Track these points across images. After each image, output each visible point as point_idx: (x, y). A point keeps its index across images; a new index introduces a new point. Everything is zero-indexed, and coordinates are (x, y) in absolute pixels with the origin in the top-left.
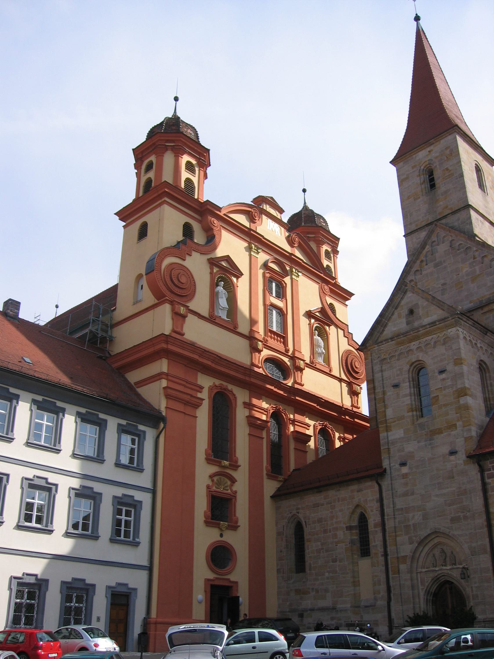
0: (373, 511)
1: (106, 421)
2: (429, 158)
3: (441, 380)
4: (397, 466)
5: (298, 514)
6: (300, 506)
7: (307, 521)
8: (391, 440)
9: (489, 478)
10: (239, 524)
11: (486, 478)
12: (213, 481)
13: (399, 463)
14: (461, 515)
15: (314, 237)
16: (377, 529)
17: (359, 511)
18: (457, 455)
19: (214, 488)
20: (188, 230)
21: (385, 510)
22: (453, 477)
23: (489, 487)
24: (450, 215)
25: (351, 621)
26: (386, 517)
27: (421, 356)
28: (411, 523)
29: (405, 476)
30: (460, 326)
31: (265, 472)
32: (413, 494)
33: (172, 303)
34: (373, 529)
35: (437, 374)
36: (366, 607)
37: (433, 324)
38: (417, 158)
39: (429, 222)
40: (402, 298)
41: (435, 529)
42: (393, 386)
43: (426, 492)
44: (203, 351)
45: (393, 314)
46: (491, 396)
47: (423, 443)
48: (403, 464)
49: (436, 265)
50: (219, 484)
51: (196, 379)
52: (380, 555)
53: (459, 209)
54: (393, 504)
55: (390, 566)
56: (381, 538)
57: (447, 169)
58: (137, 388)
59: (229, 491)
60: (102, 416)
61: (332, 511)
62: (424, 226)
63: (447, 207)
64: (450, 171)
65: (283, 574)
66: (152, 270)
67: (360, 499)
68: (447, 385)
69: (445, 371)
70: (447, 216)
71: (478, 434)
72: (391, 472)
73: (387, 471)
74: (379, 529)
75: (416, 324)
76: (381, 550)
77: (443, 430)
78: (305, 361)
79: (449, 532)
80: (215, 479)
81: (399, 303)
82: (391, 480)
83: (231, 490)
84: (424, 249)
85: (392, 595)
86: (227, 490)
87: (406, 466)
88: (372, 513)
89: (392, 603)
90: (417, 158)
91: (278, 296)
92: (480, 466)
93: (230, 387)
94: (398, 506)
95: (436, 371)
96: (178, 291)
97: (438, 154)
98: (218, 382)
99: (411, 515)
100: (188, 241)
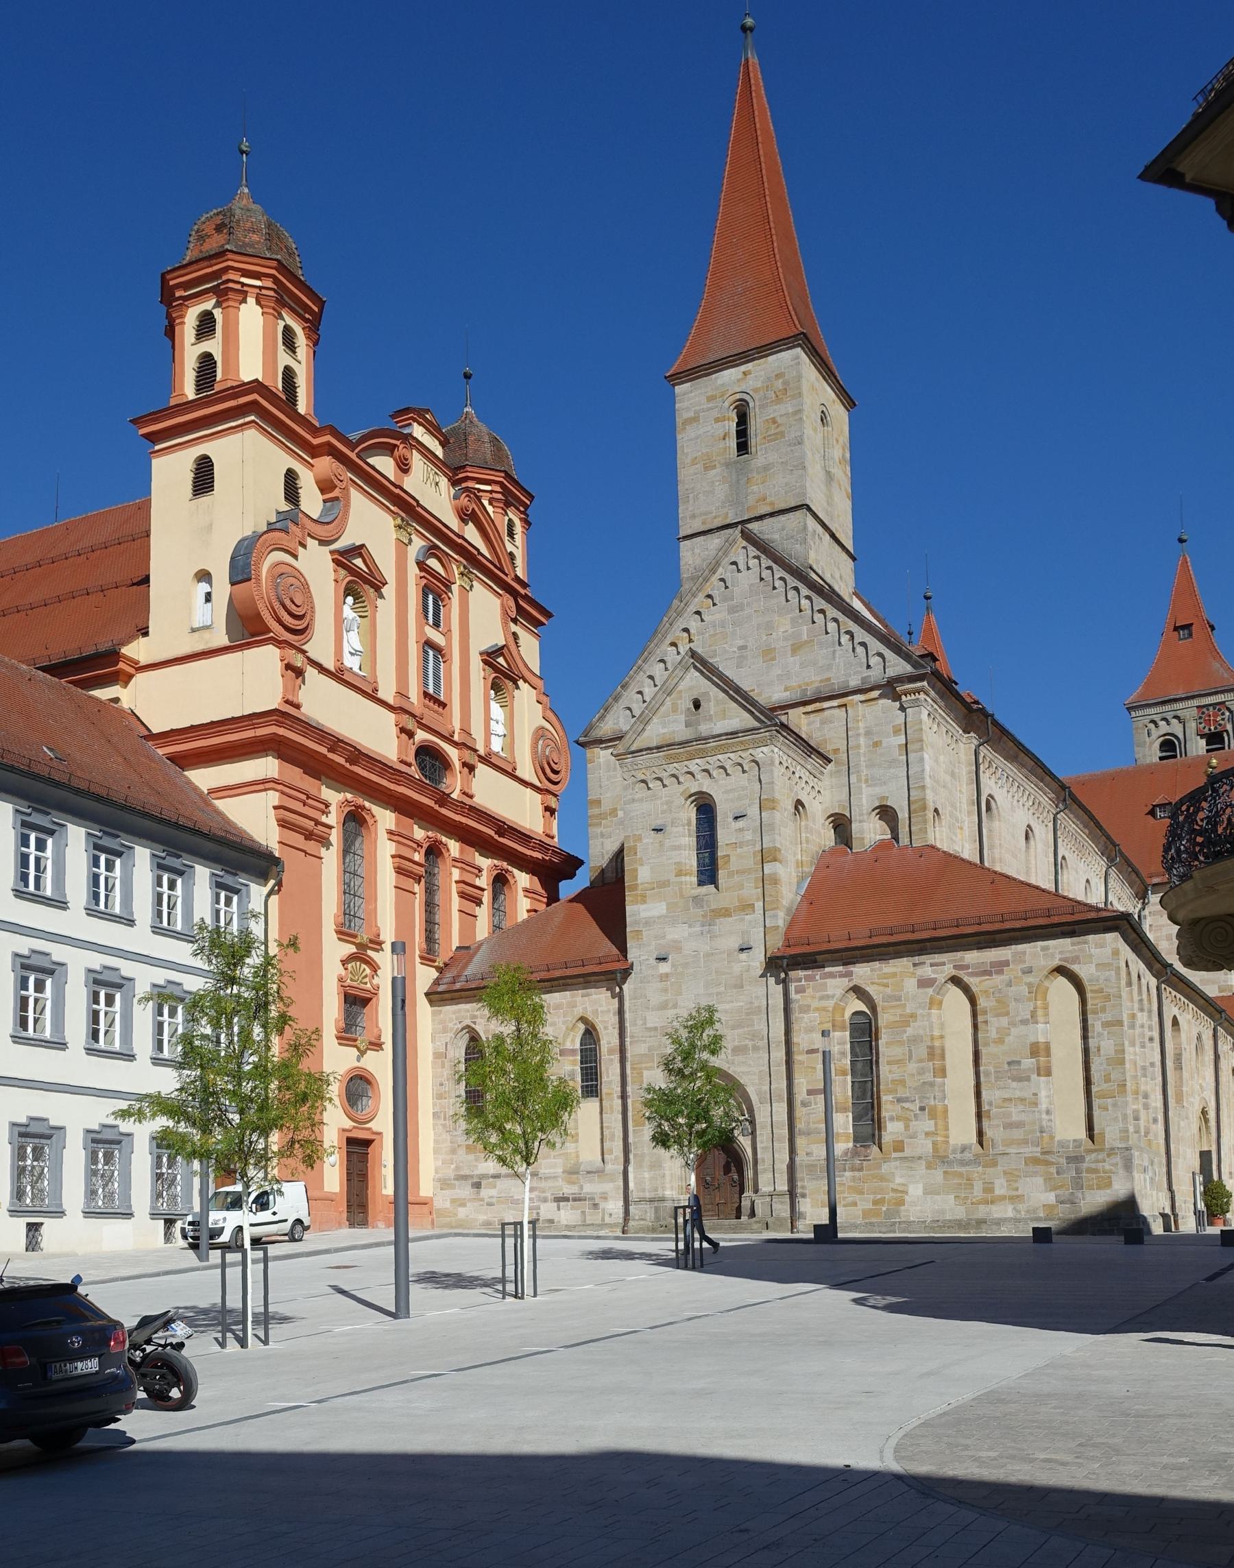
3: (736, 830)
4: (653, 961)
5: (474, 1026)
9: (797, 992)
10: (382, 1040)
12: (346, 969)
14: (750, 1044)
16: (612, 1057)
23: (794, 1006)
25: (563, 1194)
27: (706, 785)
36: (588, 1172)
37: (734, 734)
42: (653, 830)
47: (700, 929)
48: (662, 959)
52: (615, 1095)
55: (630, 1114)
56: (618, 1071)
65: (445, 1120)
74: (616, 1057)
76: (617, 1089)
79: (729, 1068)
84: (714, 573)
85: (631, 1156)
86: (366, 983)
89: (630, 1169)
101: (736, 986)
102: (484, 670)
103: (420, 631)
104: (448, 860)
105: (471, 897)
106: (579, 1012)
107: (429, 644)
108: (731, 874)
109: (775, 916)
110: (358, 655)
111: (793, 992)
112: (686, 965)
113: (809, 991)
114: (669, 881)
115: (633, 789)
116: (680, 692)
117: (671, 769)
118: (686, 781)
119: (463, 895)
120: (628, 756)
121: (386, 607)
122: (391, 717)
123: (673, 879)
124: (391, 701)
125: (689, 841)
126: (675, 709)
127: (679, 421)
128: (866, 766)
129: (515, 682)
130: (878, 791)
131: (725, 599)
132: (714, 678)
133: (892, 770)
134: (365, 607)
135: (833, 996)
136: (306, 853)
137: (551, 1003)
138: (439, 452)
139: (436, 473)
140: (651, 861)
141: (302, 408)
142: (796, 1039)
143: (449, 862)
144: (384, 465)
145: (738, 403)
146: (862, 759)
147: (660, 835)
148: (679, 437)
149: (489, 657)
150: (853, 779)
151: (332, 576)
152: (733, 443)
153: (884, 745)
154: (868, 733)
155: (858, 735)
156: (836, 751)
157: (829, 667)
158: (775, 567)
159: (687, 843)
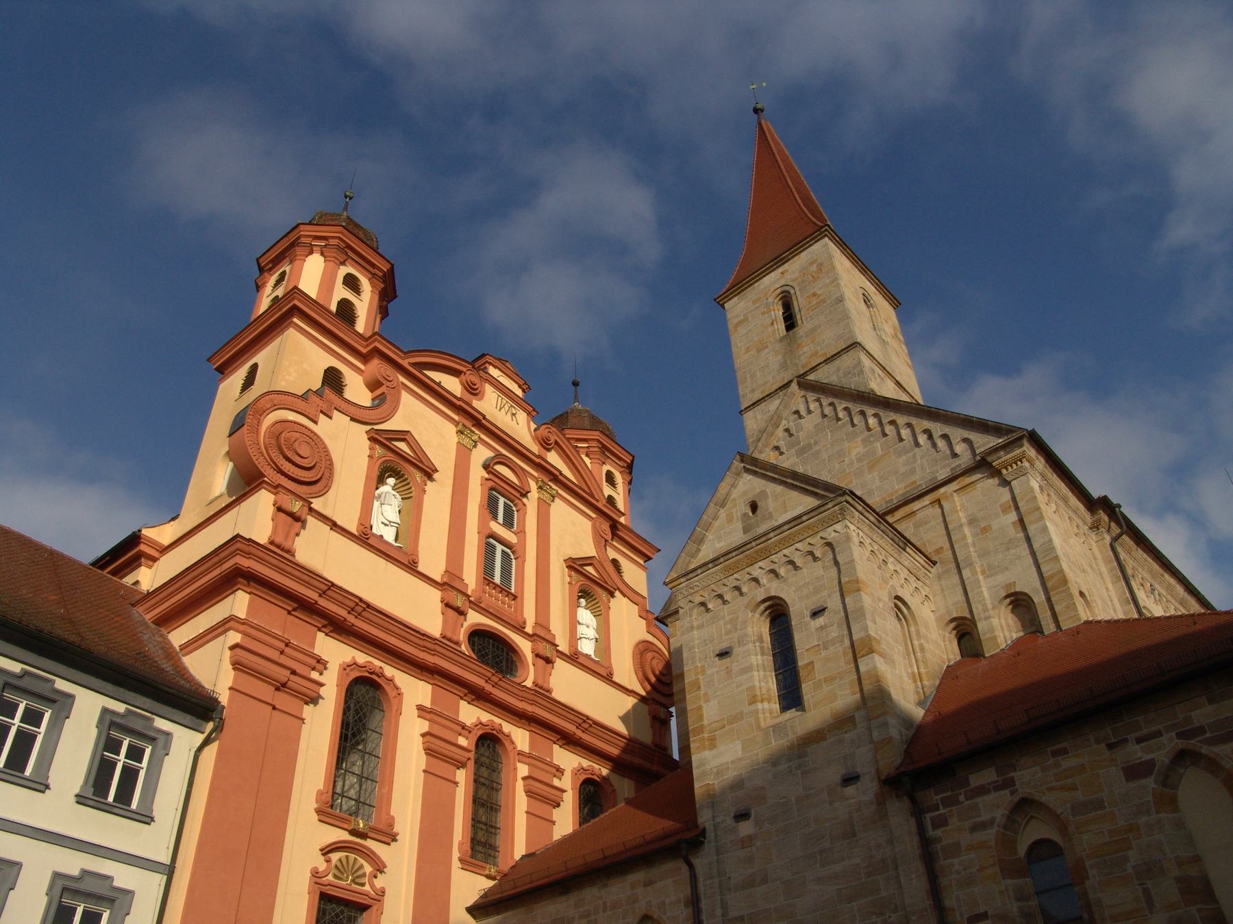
1: (71, 697)
2: (783, 282)
4: (730, 821)
8: (715, 767)
11: (930, 828)
12: (328, 861)
13: (732, 814)
15: (588, 447)
18: (859, 783)
19: (330, 877)
20: (333, 379)
22: (854, 835)
24: (823, 365)
27: (775, 588)
29: (748, 841)
30: (852, 520)
31: (456, 854)
32: (765, 881)
33: (275, 488)
35: (808, 619)
38: (762, 287)
39: (786, 382)
40: (733, 486)
44: (330, 584)
45: (715, 518)
46: (922, 670)
48: (742, 816)
49: (801, 452)
50: (340, 869)
51: (313, 645)
53: (839, 353)
54: (722, 907)
57: (814, 295)
58: (183, 656)
59: (367, 888)
60: (61, 685)
62: (776, 390)
63: (816, 353)
64: (819, 296)
66: (241, 424)
67: (650, 901)
68: (830, 638)
70: (818, 367)
71: (904, 738)
72: (716, 835)
73: (707, 835)
75: (762, 529)
77: (826, 732)
78: (558, 646)
80: (335, 857)
81: (728, 494)
82: (718, 854)
83: (372, 886)
86: (363, 885)
87: (748, 819)
90: (762, 287)
91: (508, 523)
92: (913, 800)
93: (389, 671)
95: (808, 613)
96: (296, 473)
97: (797, 275)
98: (362, 658)
100: (329, 393)
102: (570, 576)
103: (482, 524)
104: (511, 754)
105: (542, 796)
107: (493, 536)
108: (818, 686)
109: (885, 724)
111: (930, 828)
113: (954, 822)
114: (741, 712)
115: (691, 616)
116: (734, 499)
117: (731, 582)
118: (749, 590)
119: (529, 793)
120: (682, 580)
121: (437, 497)
122: (435, 595)
124: (438, 579)
125: (763, 660)
126: (730, 519)
127: (731, 327)
128: (979, 556)
130: (1001, 579)
131: (791, 446)
132: (768, 473)
133: (1012, 551)
134: (409, 484)
135: (991, 823)
136: (274, 708)
138: (519, 392)
139: (512, 406)
140: (718, 694)
141: (360, 326)
142: (949, 902)
144: (452, 384)
145: (780, 296)
146: (972, 549)
147: (726, 661)
148: (732, 338)
149: (574, 565)
150: (966, 573)
151: (368, 452)
152: (781, 326)
153: (994, 527)
154: (972, 522)
155: (961, 525)
156: (939, 551)
157: (913, 471)
158: (835, 401)
159: (760, 662)
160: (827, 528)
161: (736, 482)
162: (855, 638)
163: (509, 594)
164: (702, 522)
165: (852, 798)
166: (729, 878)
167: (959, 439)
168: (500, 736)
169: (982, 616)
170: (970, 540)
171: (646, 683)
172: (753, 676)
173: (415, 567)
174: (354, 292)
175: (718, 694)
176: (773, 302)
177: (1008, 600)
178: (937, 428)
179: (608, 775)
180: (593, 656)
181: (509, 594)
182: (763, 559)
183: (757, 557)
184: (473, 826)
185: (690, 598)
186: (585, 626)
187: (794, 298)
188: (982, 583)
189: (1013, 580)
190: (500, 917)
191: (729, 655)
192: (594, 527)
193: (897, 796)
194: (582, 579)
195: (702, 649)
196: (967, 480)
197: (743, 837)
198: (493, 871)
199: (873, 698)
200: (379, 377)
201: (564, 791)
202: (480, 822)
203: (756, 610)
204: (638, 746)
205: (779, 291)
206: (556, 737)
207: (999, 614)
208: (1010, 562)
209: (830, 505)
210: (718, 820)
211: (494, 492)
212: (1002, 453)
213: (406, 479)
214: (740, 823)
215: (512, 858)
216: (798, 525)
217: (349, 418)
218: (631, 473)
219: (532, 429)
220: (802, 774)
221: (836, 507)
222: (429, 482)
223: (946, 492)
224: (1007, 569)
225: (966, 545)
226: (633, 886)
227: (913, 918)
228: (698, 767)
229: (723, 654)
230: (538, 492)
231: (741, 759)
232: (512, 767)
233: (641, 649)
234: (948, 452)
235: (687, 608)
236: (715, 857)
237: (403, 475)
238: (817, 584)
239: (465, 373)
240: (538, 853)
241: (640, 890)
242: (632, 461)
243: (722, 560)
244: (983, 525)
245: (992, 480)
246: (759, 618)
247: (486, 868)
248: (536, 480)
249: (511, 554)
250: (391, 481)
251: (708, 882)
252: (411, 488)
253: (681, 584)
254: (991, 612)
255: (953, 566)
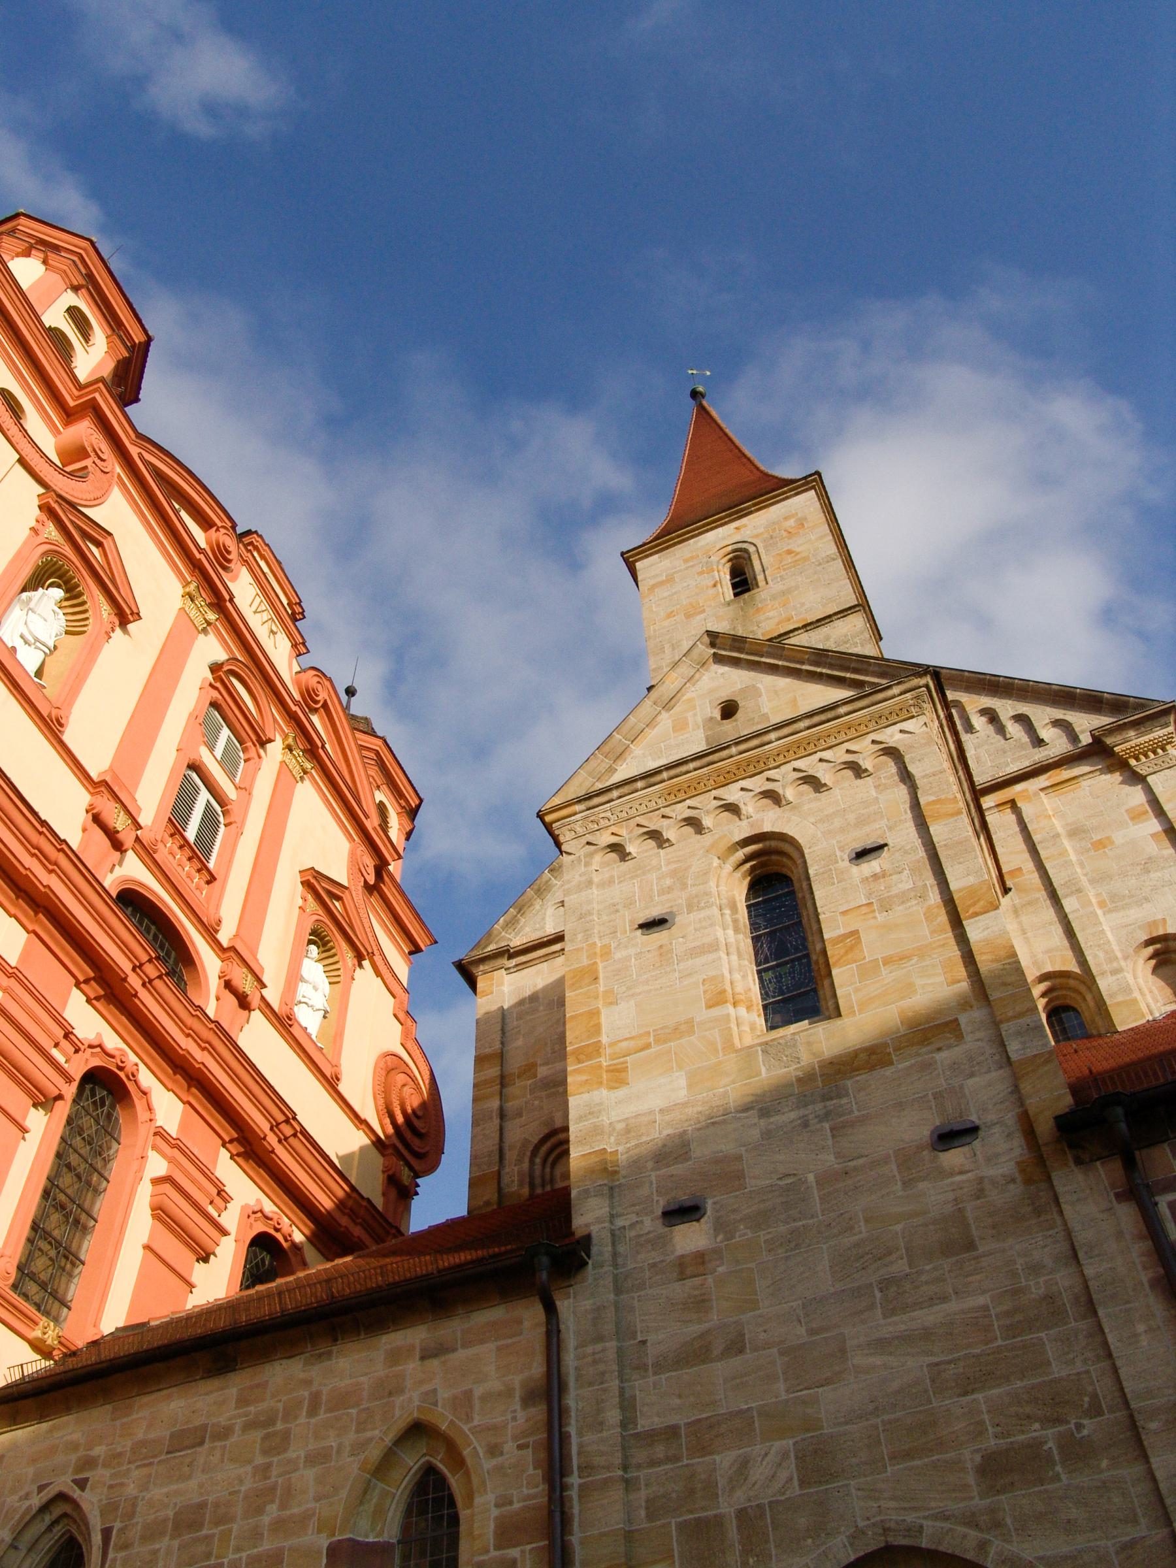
0: (502, 1454)
2: (738, 538)
4: (651, 1224)
6: (99, 1451)
7: (117, 1525)
14: (1050, 1436)
16: (514, 1552)
17: (412, 1461)
18: (977, 1144)
21: (574, 1441)
22: (971, 1246)
24: (800, 632)
26: (574, 1480)
27: (770, 820)
28: (726, 1507)
32: (736, 1346)
34: (494, 1553)
38: (700, 544)
41: (886, 1530)
43: (812, 1332)
45: (650, 724)
47: (793, 1115)
53: (829, 616)
61: (267, 1467)
64: (798, 554)
67: (435, 1391)
68: (894, 891)
69: (881, 847)
73: (594, 1250)
79: (982, 1546)
82: (618, 1291)
87: (698, 1220)
88: (494, 1462)
90: (700, 544)
92: (1130, 1164)
94: (643, 1424)
95: (845, 855)
99: (724, 1460)
101: (948, 1249)
106: (406, 1407)
108: (869, 970)
110: (37, 648)
112: (759, 1220)
115: (587, 864)
116: (689, 700)
120: (577, 808)
123: (703, 1014)
129: (360, 957)
132: (763, 660)
133: (1155, 875)
134: (86, 611)
137: (325, 1391)
143: (144, 1132)
147: (658, 937)
150: (1069, 904)
160: (885, 727)
161: (697, 676)
162: (953, 886)
163: (203, 868)
164: (625, 728)
165: (961, 1173)
166: (644, 1342)
167: (1047, 721)
168: (130, 1086)
169: (1106, 967)
170: (1073, 857)
171: (387, 1121)
172: (720, 958)
173: (59, 731)
174: (80, 331)
175: (637, 991)
176: (718, 562)
177: (1150, 950)
178: (1006, 708)
179: (301, 1243)
180: (314, 1037)
181: (203, 868)
182: (751, 776)
183: (736, 772)
184: (30, 1241)
185: (589, 838)
186: (310, 987)
187: (755, 558)
188: (1102, 918)
189: (1159, 917)
190: (45, 1426)
191: (667, 925)
192: (352, 854)
193: (1079, 1162)
194: (321, 912)
195: (605, 918)
196: (1065, 774)
197: (682, 1256)
198: (51, 1338)
199: (1004, 984)
200: (86, 444)
201: (224, 1232)
202: (33, 1277)
203: (727, 858)
204: (365, 1203)
205: (730, 548)
206: (228, 1133)
207: (1134, 970)
208: (1152, 890)
209: (896, 690)
210: (620, 1222)
211: (194, 776)
212: (1132, 733)
213: (84, 603)
214: (677, 1228)
215: (96, 1325)
216: (829, 721)
217: (17, 457)
218: (413, 819)
219: (294, 671)
220: (832, 1130)
221: (907, 695)
222: (118, 630)
223: (1027, 790)
224: (1147, 899)
225: (1068, 864)
226: (394, 1357)
227: (1153, 1426)
228: (580, 1118)
229: (652, 925)
230: (283, 754)
231: (684, 1105)
232: (138, 1152)
233: (389, 1064)
234: (1026, 739)
235: (582, 853)
236: (612, 1296)
237: (80, 594)
238: (862, 811)
239: (218, 530)
240: (153, 1323)
241: (412, 1367)
242: (418, 807)
243: (665, 775)
244: (1096, 838)
245: (1108, 776)
246: (730, 874)
247: (36, 1324)
248: (286, 737)
249: (220, 813)
250: (58, 593)
251: (589, 1350)
252: (87, 619)
253: (575, 814)
254: (1123, 963)
255: (1042, 895)
